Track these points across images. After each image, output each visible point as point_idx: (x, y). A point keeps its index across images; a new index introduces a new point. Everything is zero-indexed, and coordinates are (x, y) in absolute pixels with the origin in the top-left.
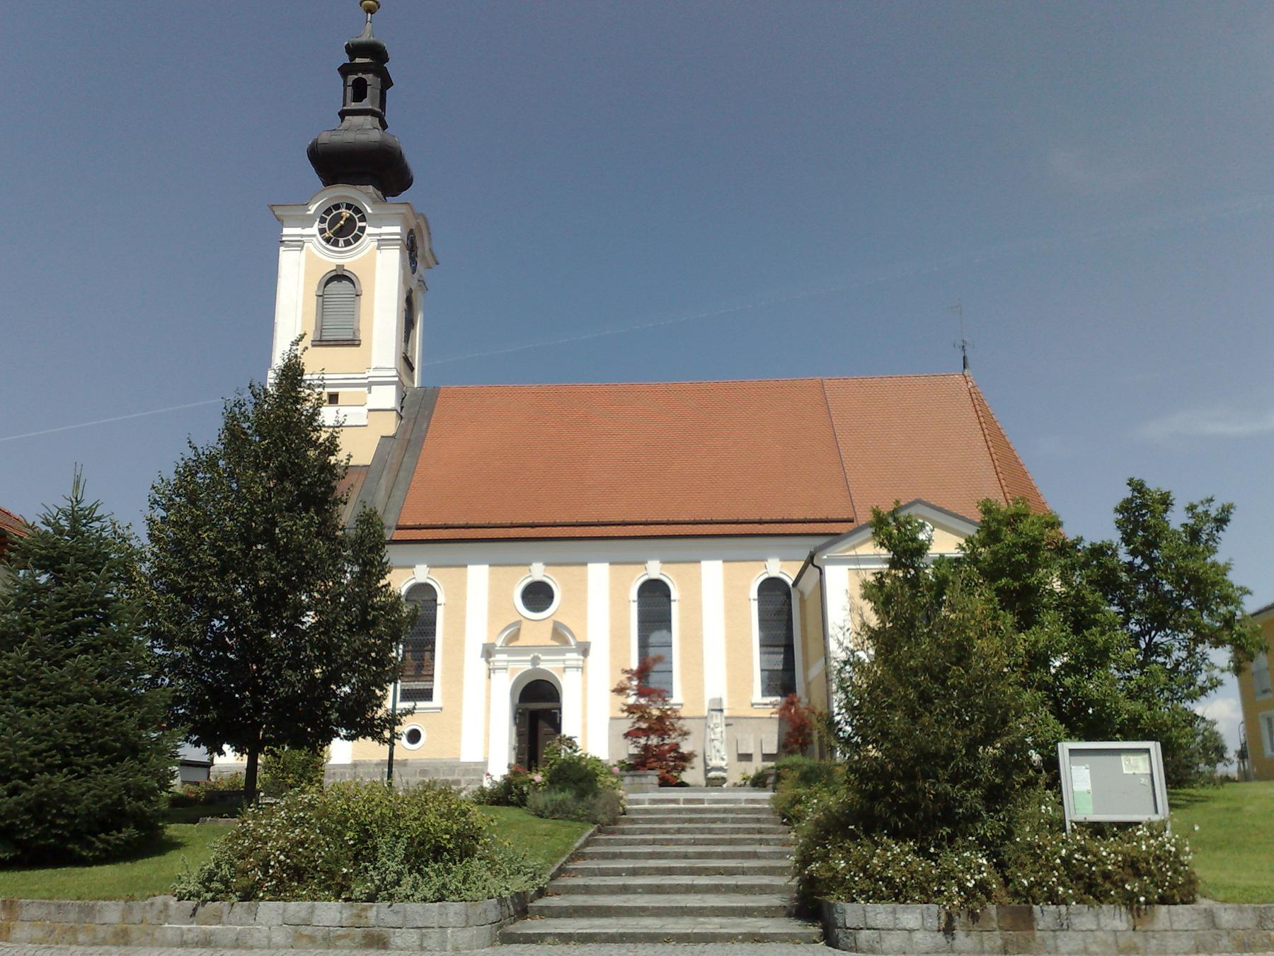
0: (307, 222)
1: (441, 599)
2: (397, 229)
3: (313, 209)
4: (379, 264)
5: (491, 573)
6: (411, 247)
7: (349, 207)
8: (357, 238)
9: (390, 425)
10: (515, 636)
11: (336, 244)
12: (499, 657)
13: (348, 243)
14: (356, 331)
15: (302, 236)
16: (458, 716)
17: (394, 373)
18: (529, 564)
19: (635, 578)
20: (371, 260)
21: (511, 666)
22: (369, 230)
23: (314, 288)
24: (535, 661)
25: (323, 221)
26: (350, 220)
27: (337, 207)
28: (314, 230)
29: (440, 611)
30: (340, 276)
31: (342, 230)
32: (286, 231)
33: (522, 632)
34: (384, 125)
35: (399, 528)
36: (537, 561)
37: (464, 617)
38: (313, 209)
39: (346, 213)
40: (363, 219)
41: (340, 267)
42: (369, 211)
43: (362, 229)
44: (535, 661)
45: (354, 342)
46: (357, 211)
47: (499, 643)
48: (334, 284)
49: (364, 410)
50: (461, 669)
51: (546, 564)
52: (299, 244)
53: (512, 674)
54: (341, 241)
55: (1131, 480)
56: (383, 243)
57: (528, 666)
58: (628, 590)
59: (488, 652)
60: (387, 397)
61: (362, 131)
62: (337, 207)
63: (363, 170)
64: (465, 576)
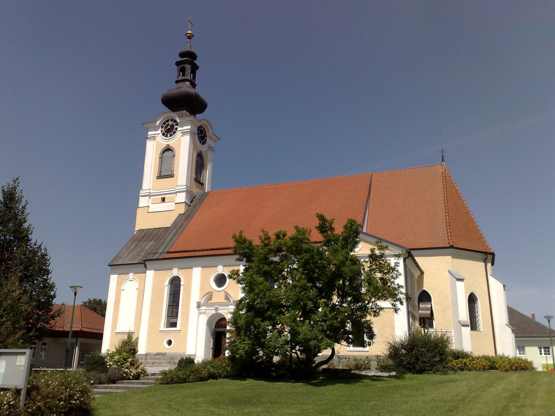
0: (156, 129)
1: (182, 283)
2: (189, 127)
3: (158, 123)
4: (183, 143)
5: (202, 271)
6: (201, 135)
7: (172, 120)
8: (174, 133)
9: (182, 209)
10: (210, 298)
11: (167, 136)
12: (203, 308)
13: (171, 135)
14: (172, 171)
15: (155, 134)
16: (186, 334)
17: (185, 187)
18: (217, 266)
19: (167, 277)
20: (180, 140)
21: (207, 312)
22: (179, 129)
23: (158, 155)
24: (217, 309)
25: (162, 127)
26: (172, 126)
27: (168, 121)
28: (159, 132)
29: (182, 287)
30: (168, 149)
31: (169, 131)
32: (149, 133)
33: (213, 297)
34: (194, 85)
35: (168, 253)
36: (220, 265)
37: (190, 290)
38: (158, 123)
39: (170, 123)
40: (177, 125)
41: (168, 145)
42: (178, 121)
43: (176, 129)
44: (217, 309)
45: (171, 176)
46: (175, 121)
47: (202, 302)
48: (166, 153)
49: (173, 203)
50: (188, 313)
51: (224, 266)
52: (154, 138)
53: (207, 316)
54: (169, 134)
55: (201, 127)
56: (184, 133)
57: (214, 312)
58: (209, 280)
59: (199, 306)
60: (182, 197)
61: (186, 87)
62: (168, 121)
63: (185, 103)
64: (192, 272)
